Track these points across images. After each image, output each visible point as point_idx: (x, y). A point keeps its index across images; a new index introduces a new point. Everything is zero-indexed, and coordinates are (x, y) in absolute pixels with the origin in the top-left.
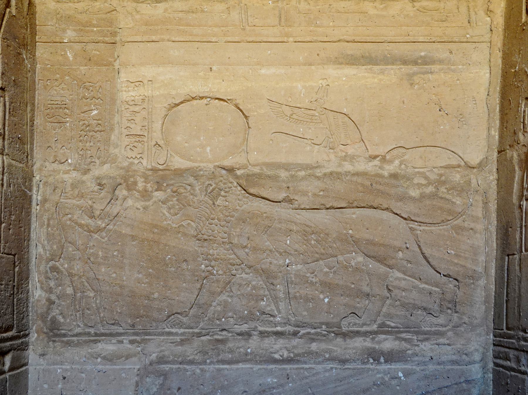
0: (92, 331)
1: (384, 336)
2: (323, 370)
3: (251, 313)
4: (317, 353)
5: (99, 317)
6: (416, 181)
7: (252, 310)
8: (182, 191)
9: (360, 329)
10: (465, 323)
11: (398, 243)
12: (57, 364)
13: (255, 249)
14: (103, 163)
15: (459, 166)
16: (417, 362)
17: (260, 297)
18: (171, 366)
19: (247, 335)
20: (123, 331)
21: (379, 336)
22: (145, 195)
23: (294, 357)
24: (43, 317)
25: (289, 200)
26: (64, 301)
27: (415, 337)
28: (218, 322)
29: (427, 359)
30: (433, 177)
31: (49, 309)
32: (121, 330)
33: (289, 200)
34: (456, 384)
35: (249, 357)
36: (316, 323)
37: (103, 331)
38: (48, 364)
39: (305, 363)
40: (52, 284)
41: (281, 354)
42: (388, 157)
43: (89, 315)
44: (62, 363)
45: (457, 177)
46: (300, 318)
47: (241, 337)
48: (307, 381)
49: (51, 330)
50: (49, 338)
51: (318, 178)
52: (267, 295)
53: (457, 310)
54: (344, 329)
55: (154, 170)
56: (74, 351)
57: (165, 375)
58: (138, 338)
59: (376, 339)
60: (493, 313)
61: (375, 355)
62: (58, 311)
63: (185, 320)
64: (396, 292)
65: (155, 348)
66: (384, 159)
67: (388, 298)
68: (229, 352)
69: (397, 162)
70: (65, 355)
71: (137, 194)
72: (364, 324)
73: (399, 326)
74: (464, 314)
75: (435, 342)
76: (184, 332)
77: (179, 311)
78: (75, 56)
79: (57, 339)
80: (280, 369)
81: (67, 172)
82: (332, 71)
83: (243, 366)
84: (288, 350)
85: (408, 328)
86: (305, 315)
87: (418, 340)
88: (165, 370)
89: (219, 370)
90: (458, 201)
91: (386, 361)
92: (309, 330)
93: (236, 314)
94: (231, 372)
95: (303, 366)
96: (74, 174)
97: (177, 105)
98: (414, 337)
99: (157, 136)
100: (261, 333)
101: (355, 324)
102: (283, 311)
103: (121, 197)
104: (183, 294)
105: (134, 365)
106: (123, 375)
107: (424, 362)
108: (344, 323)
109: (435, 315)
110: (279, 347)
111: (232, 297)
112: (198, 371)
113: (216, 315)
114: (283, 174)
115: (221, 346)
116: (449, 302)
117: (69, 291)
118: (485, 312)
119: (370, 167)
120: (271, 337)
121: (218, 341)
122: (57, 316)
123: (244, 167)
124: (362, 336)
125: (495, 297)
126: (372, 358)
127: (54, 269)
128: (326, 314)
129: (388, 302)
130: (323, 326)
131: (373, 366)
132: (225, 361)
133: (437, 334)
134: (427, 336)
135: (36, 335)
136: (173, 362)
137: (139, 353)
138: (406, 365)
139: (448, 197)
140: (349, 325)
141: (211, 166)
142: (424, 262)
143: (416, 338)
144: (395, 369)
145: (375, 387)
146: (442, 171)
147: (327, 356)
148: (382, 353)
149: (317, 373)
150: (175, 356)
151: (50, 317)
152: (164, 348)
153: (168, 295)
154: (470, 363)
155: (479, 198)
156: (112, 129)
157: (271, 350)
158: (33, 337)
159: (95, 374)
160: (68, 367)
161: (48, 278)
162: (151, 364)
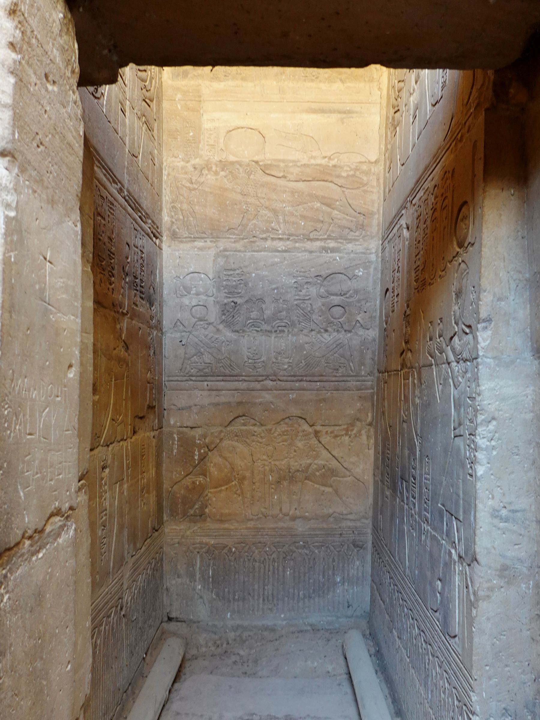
0: (192, 236)
1: (329, 241)
3: (267, 229)
6: (345, 169)
8: (234, 171)
11: (337, 198)
13: (269, 199)
14: (196, 158)
15: (366, 162)
19: (265, 239)
22: (216, 173)
24: (169, 229)
25: (284, 177)
27: (345, 242)
29: (350, 251)
30: (353, 167)
31: (172, 225)
32: (206, 236)
33: (284, 177)
39: (293, 252)
40: (173, 214)
42: (332, 157)
44: (178, 250)
45: (365, 167)
50: (172, 239)
51: (299, 167)
55: (220, 161)
57: (227, 257)
58: (214, 240)
61: (325, 249)
63: (236, 232)
64: (335, 220)
65: (222, 244)
66: (330, 158)
69: (336, 160)
71: (212, 173)
72: (320, 236)
78: (181, 107)
81: (179, 162)
82: (305, 116)
85: (341, 237)
89: (252, 255)
90: (365, 178)
91: (331, 252)
96: (182, 163)
97: (230, 131)
99: (222, 145)
100: (272, 238)
103: (204, 174)
105: (212, 252)
110: (281, 245)
114: (282, 165)
115: (253, 244)
117: (181, 217)
119: (324, 162)
121: (251, 242)
123: (263, 161)
127: (173, 207)
134: (350, 241)
136: (231, 251)
139: (361, 176)
141: (247, 160)
142: (349, 207)
146: (358, 164)
148: (329, 248)
154: (370, 253)
155: (375, 177)
156: (200, 142)
158: (164, 238)
161: (171, 211)
162: (220, 252)
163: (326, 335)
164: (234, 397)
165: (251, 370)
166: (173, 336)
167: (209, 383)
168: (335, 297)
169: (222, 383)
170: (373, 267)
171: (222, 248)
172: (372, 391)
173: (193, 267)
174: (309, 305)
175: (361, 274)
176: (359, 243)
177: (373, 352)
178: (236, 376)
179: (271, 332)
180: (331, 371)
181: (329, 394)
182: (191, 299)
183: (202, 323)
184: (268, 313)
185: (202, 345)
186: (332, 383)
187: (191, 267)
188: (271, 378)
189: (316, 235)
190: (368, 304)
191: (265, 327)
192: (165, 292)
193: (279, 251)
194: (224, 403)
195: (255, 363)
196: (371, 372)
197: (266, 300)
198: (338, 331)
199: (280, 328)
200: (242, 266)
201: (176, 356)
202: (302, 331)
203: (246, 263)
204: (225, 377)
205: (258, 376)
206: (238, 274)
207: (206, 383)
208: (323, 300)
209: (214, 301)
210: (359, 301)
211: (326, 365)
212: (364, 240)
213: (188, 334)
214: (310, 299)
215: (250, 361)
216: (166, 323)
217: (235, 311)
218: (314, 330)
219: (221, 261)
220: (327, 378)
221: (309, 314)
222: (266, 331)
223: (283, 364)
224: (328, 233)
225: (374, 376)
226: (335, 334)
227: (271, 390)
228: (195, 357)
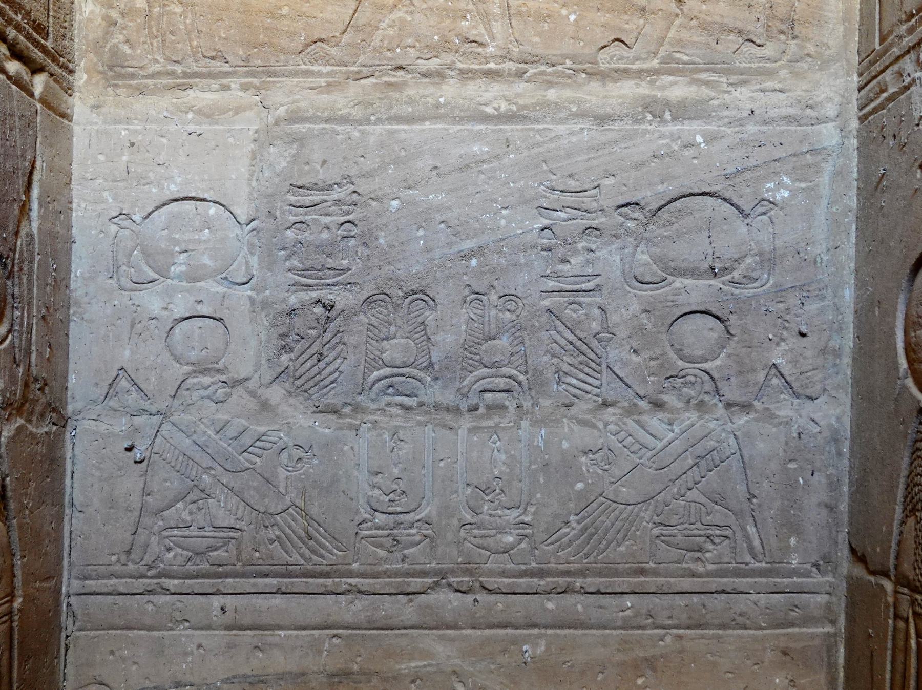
0: (179, 69)
1: (671, 78)
2: (567, 132)
3: (445, 40)
4: (556, 104)
5: (191, 46)
7: (446, 33)
9: (630, 66)
10: (808, 55)
12: (119, 122)
16: (727, 120)
17: (460, 13)
18: (312, 126)
20: (230, 69)
21: (663, 77)
23: (518, 110)
26: (132, 21)
27: (724, 80)
28: (389, 54)
29: (745, 114)
32: (226, 68)
34: (795, 155)
35: (442, 111)
36: (554, 55)
37: (196, 69)
38: (104, 122)
39: (537, 121)
41: (497, 106)
43: (172, 42)
44: (128, 121)
46: (528, 48)
47: (427, 80)
48: (541, 149)
49: (111, 68)
50: (107, 80)
52: (472, 11)
53: (796, 32)
54: (603, 67)
56: (149, 101)
57: (299, 140)
58: (255, 81)
59: (657, 83)
60: (857, 39)
61: (654, 109)
62: (121, 37)
63: (333, 51)
67: (677, 15)
68: (407, 103)
70: (134, 107)
72: (637, 59)
73: (696, 60)
74: (807, 39)
75: (758, 86)
76: (332, 71)
77: (324, 36)
79: (120, 83)
80: (493, 131)
83: (432, 126)
84: (507, 100)
86: (537, 43)
87: (730, 84)
88: (301, 132)
89: (391, 133)
91: (674, 119)
92: (543, 68)
93: (418, 41)
94: (412, 135)
95: (533, 126)
98: (721, 80)
100: (462, 72)
101: (621, 58)
102: (498, 36)
104: (330, 8)
105: (249, 123)
106: (231, 140)
107: (739, 120)
108: (603, 55)
109: (758, 42)
111: (412, 13)
112: (357, 134)
113: (386, 42)
115: (395, 95)
116: (782, 21)
118: (844, 36)
120: (479, 81)
121: (389, 84)
122: (120, 46)
124: (633, 78)
125: (861, 10)
126: (651, 112)
128: (572, 41)
129: (677, 22)
130: (567, 61)
131: (653, 127)
132: (402, 117)
133: (761, 74)
134: (744, 77)
135: (85, 77)
136: (313, 119)
137: (256, 105)
138: (709, 124)
140: (611, 59)
143: (725, 81)
144: (689, 130)
145: (656, 160)
147: (574, 109)
148: (668, 104)
149: (558, 137)
150: (317, 109)
151: (108, 46)
152: (299, 97)
153: (304, 9)
154: (819, 121)
157: (479, 99)
158: (80, 79)
159: (184, 138)
160: (139, 127)
162: (277, 123)
163: (655, 422)
164: (320, 652)
165: (382, 553)
166: (103, 427)
167: (229, 601)
168: (688, 282)
169: (278, 600)
170: (828, 168)
171: (282, 111)
172: (829, 629)
173: (178, 180)
174: (596, 312)
175: (786, 194)
176: (778, 86)
177: (833, 485)
178: (327, 575)
179: (455, 410)
180: (675, 553)
181: (668, 639)
182: (169, 293)
183: (206, 380)
184: (447, 341)
185: (206, 462)
186: (680, 601)
187: (170, 179)
188: (453, 580)
189: (621, 58)
190: (812, 307)
191: (436, 393)
192: (79, 269)
193: (486, 118)
194: (281, 676)
195: (398, 524)
196: (827, 559)
197: (440, 293)
198: (701, 406)
199: (488, 396)
200: (354, 171)
201: (112, 503)
202: (569, 405)
203: (369, 164)
204: (288, 578)
205: (408, 574)
206: (338, 202)
207: (216, 602)
208: (648, 293)
209: (252, 301)
210: (780, 292)
211: (656, 531)
212: (796, 75)
213: (156, 420)
214: (598, 288)
215: (380, 519)
216: (80, 384)
217: (327, 336)
218: (612, 404)
219: (279, 157)
220: (661, 580)
221: (594, 343)
222: (437, 407)
223: (501, 530)
224: (662, 53)
225: (834, 572)
226: (693, 416)
227: (456, 627)
228: (180, 505)
